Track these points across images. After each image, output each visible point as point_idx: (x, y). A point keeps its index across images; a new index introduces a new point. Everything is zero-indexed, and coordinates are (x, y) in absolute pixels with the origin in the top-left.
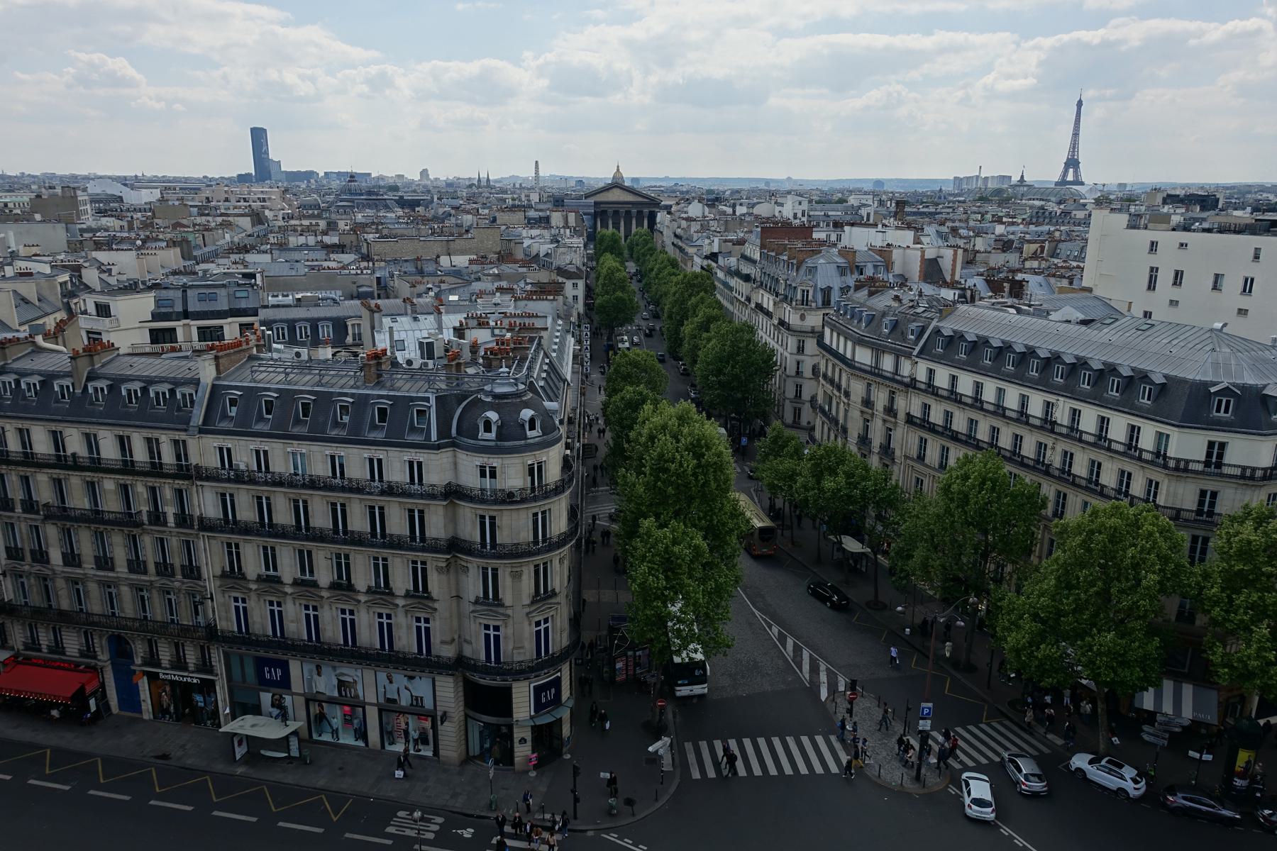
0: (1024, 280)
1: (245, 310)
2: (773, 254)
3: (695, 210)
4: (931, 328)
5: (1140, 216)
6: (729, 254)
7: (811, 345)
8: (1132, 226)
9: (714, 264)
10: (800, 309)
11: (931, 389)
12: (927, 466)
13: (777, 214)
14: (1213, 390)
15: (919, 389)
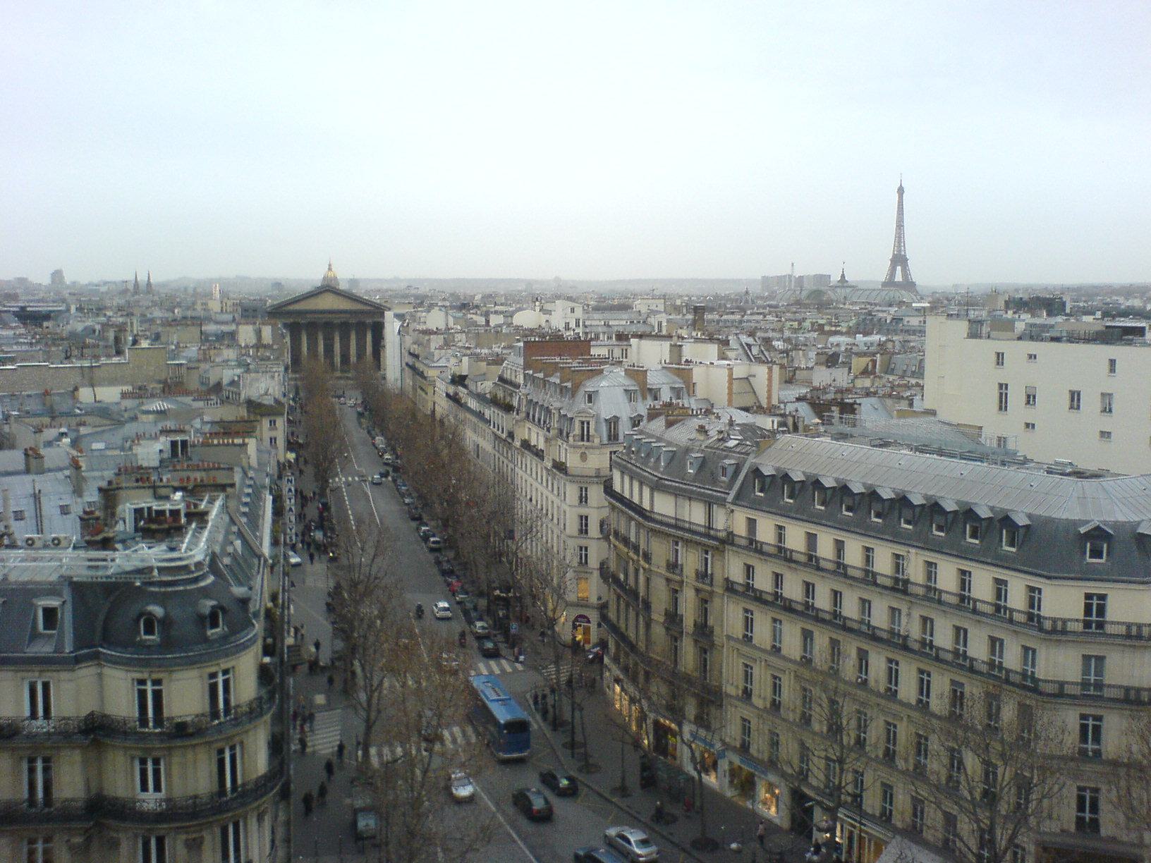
0: (855, 403)
2: (541, 375)
3: (435, 319)
5: (981, 322)
6: (484, 377)
7: (596, 494)
8: (973, 335)
9: (462, 391)
10: (580, 447)
11: (754, 546)
12: (755, 647)
13: (544, 324)
14: (1083, 530)
15: (739, 546)
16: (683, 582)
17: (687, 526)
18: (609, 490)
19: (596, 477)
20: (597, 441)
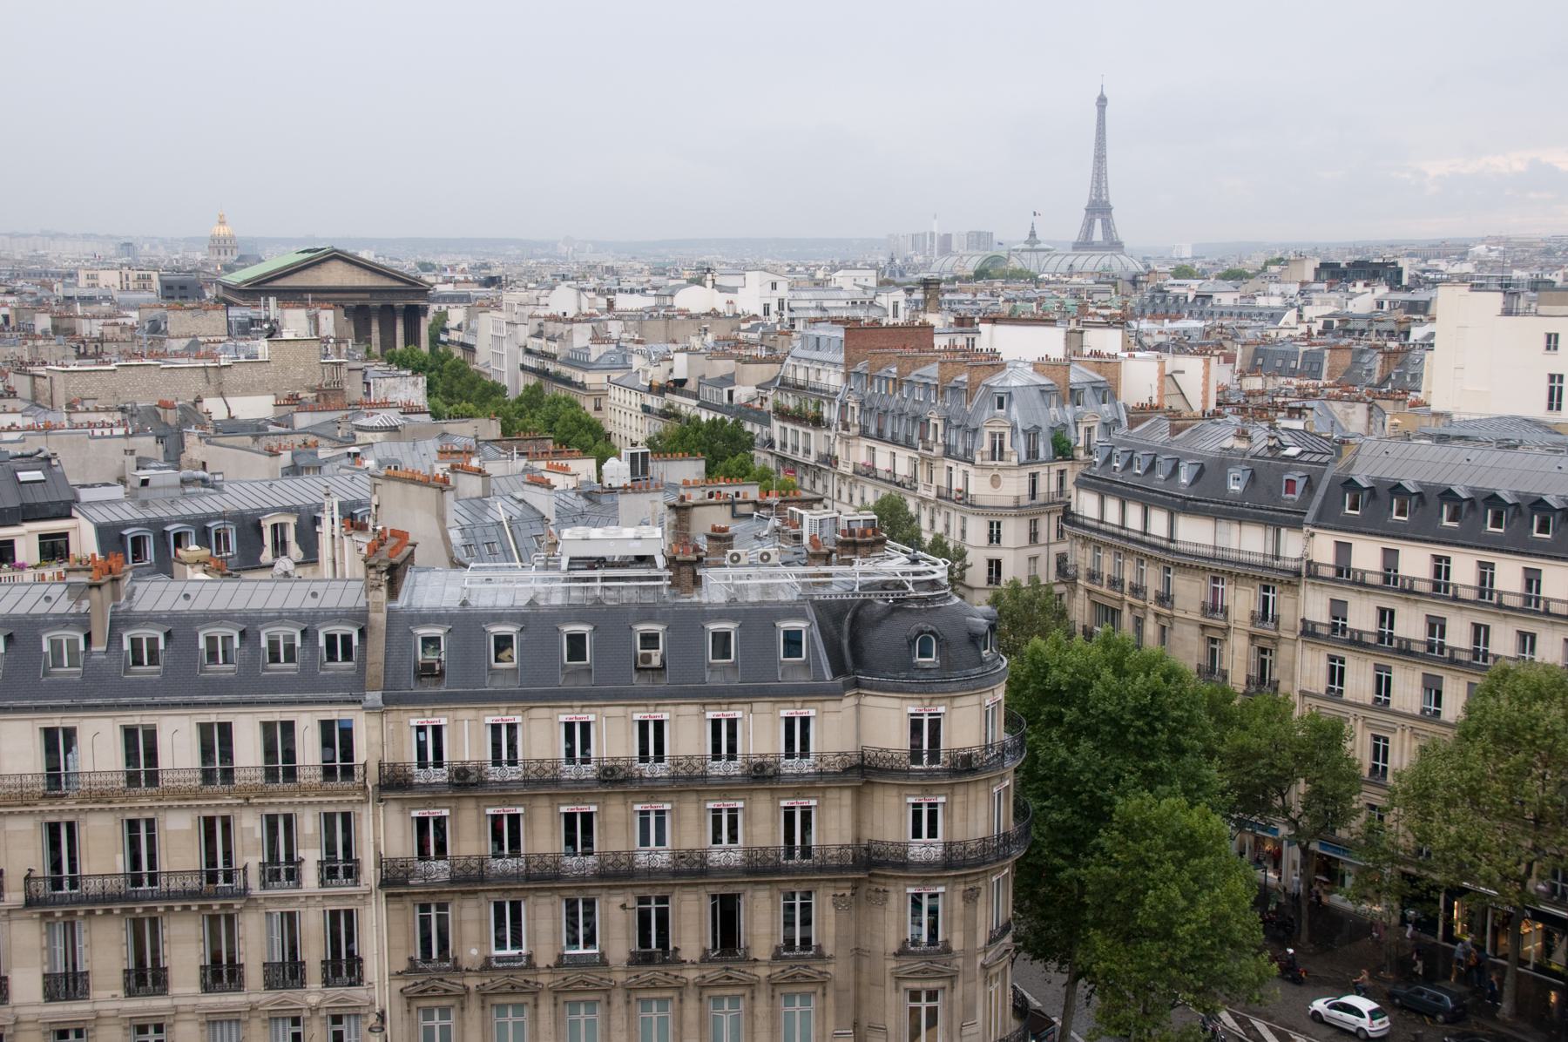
1: (43, 506)
3: (564, 300)
4: (1327, 478)
8: (1507, 312)
10: (990, 468)
16: (1229, 627)
17: (1234, 556)
18: (1068, 516)
19: (1014, 508)
20: (1014, 460)
